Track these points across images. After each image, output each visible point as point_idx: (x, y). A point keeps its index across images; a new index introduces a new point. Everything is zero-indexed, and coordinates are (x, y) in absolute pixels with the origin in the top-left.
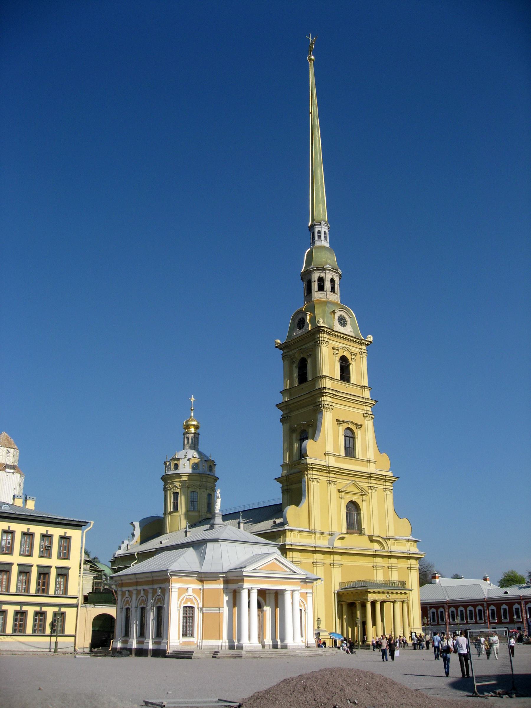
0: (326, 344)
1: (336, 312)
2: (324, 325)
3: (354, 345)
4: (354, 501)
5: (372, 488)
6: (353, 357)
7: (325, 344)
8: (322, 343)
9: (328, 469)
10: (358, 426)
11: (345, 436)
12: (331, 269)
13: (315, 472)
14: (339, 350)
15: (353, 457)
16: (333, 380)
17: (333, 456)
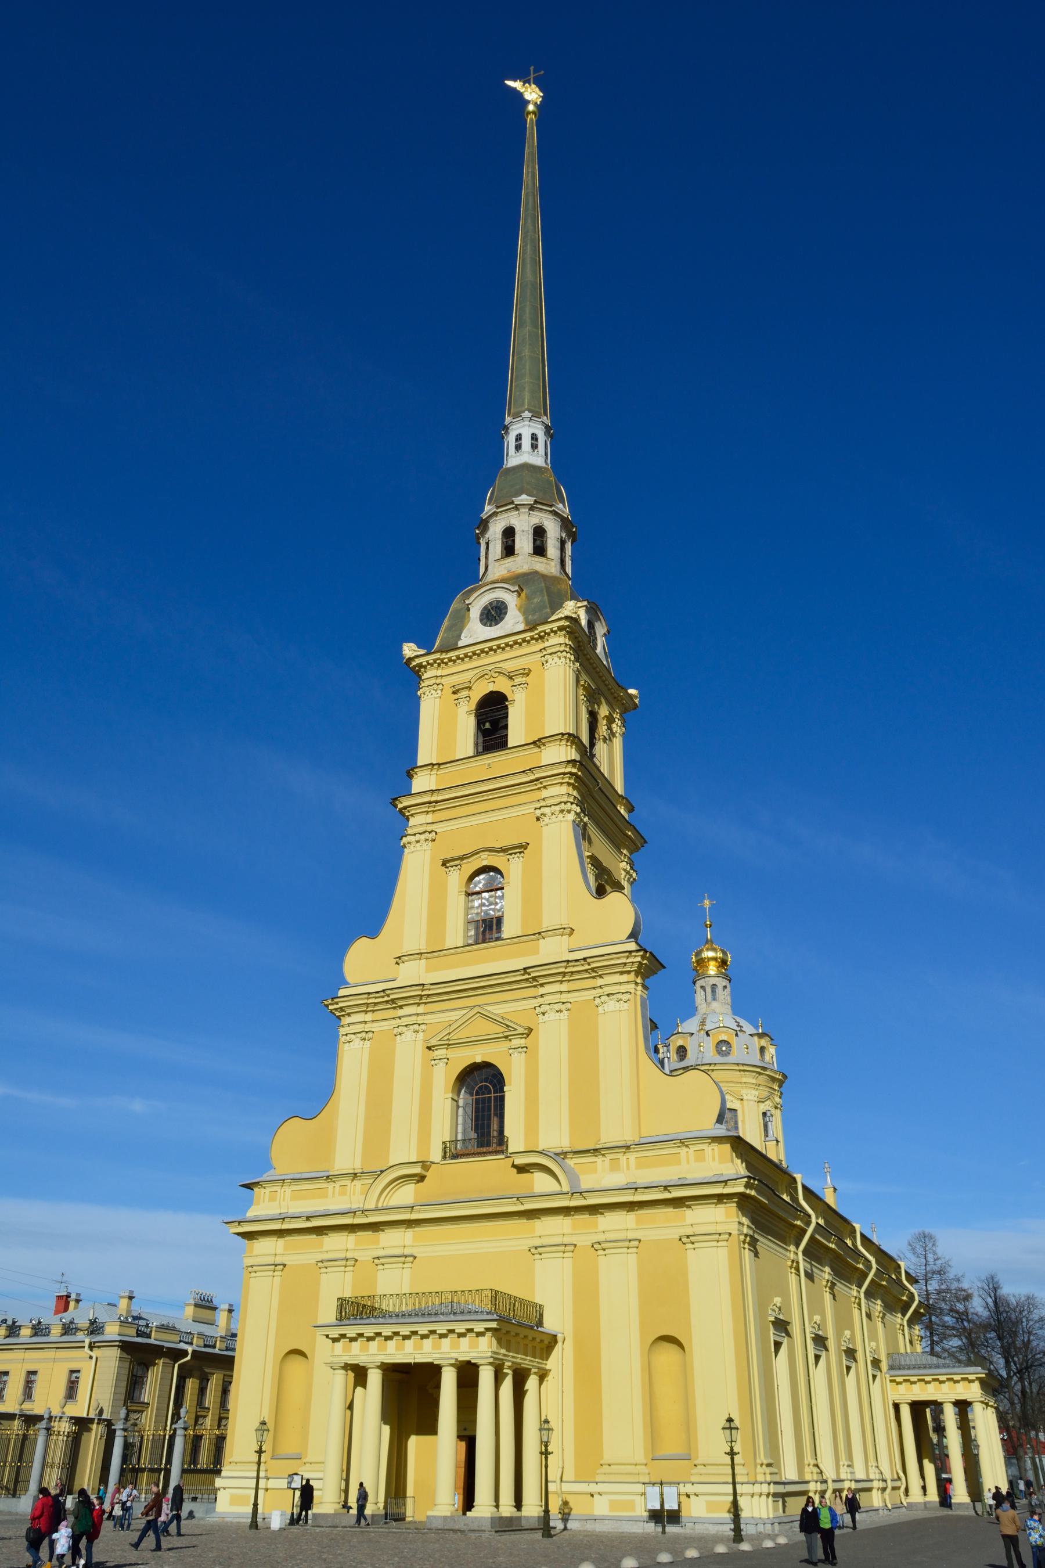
0: (433, 692)
1: (470, 604)
2: (416, 654)
3: (517, 651)
4: (483, 1062)
5: (543, 1009)
6: (518, 680)
7: (427, 693)
8: (422, 695)
9: (386, 999)
10: (510, 852)
11: (468, 894)
12: (495, 510)
13: (355, 1018)
14: (470, 688)
15: (480, 942)
16: (442, 767)
17: (420, 959)
